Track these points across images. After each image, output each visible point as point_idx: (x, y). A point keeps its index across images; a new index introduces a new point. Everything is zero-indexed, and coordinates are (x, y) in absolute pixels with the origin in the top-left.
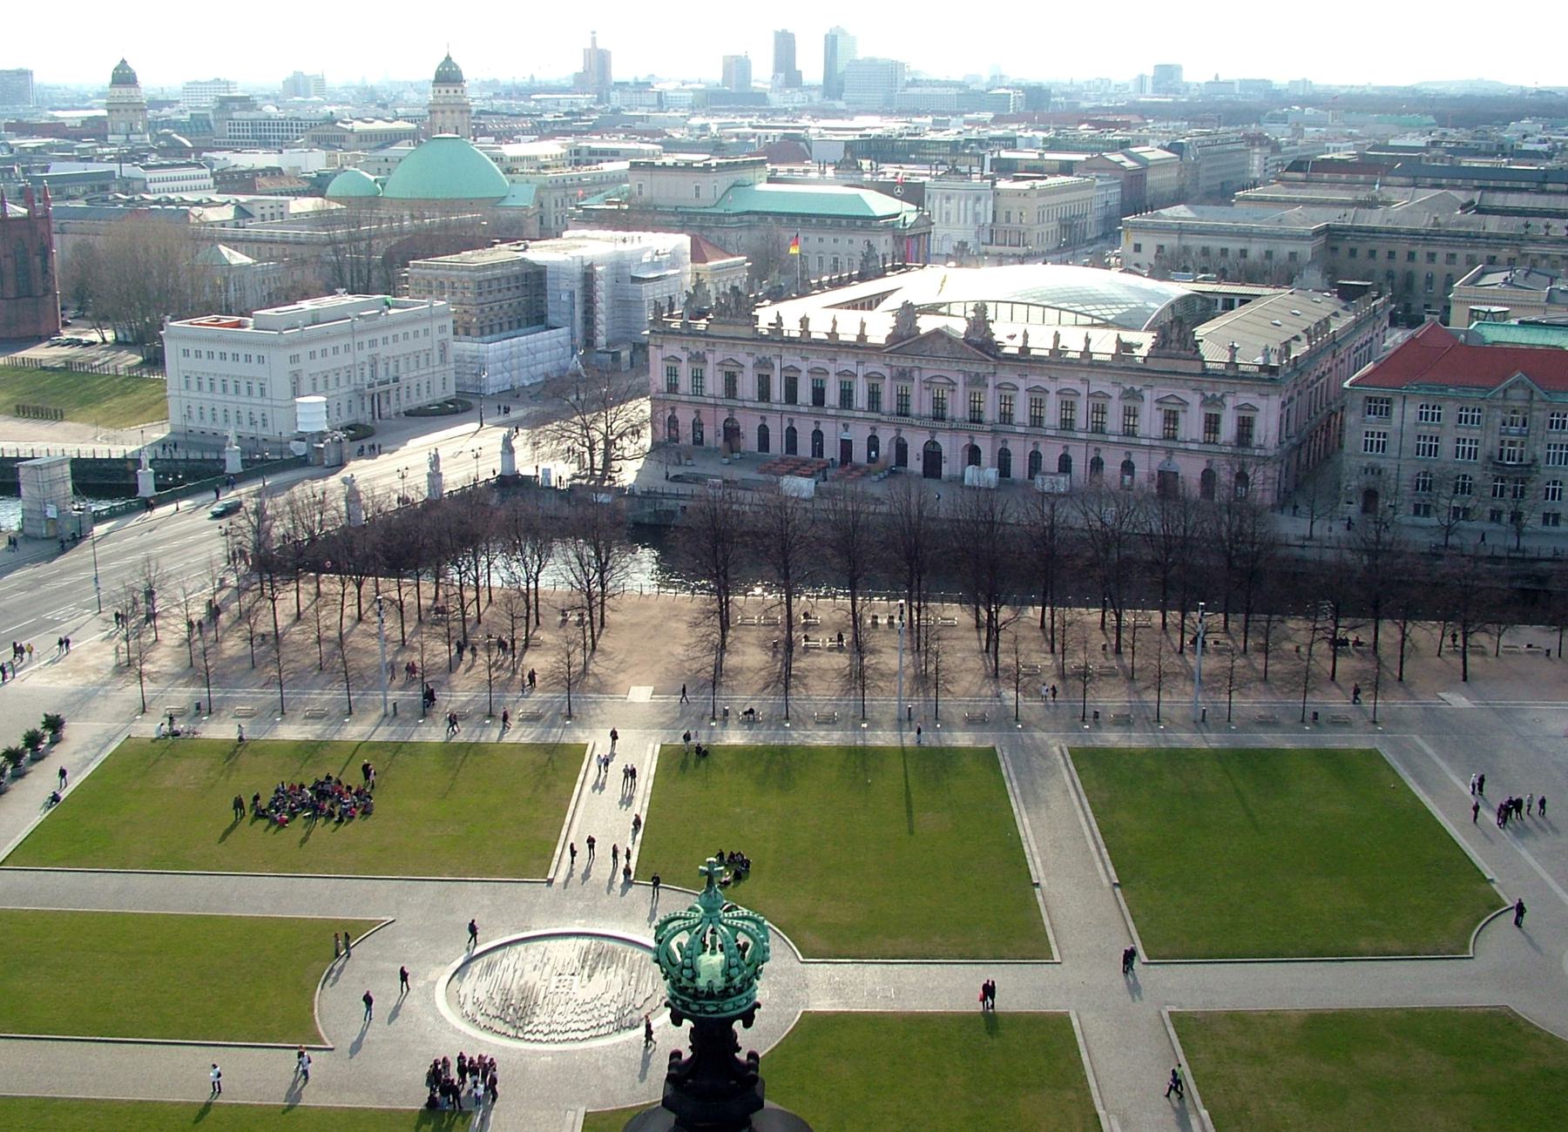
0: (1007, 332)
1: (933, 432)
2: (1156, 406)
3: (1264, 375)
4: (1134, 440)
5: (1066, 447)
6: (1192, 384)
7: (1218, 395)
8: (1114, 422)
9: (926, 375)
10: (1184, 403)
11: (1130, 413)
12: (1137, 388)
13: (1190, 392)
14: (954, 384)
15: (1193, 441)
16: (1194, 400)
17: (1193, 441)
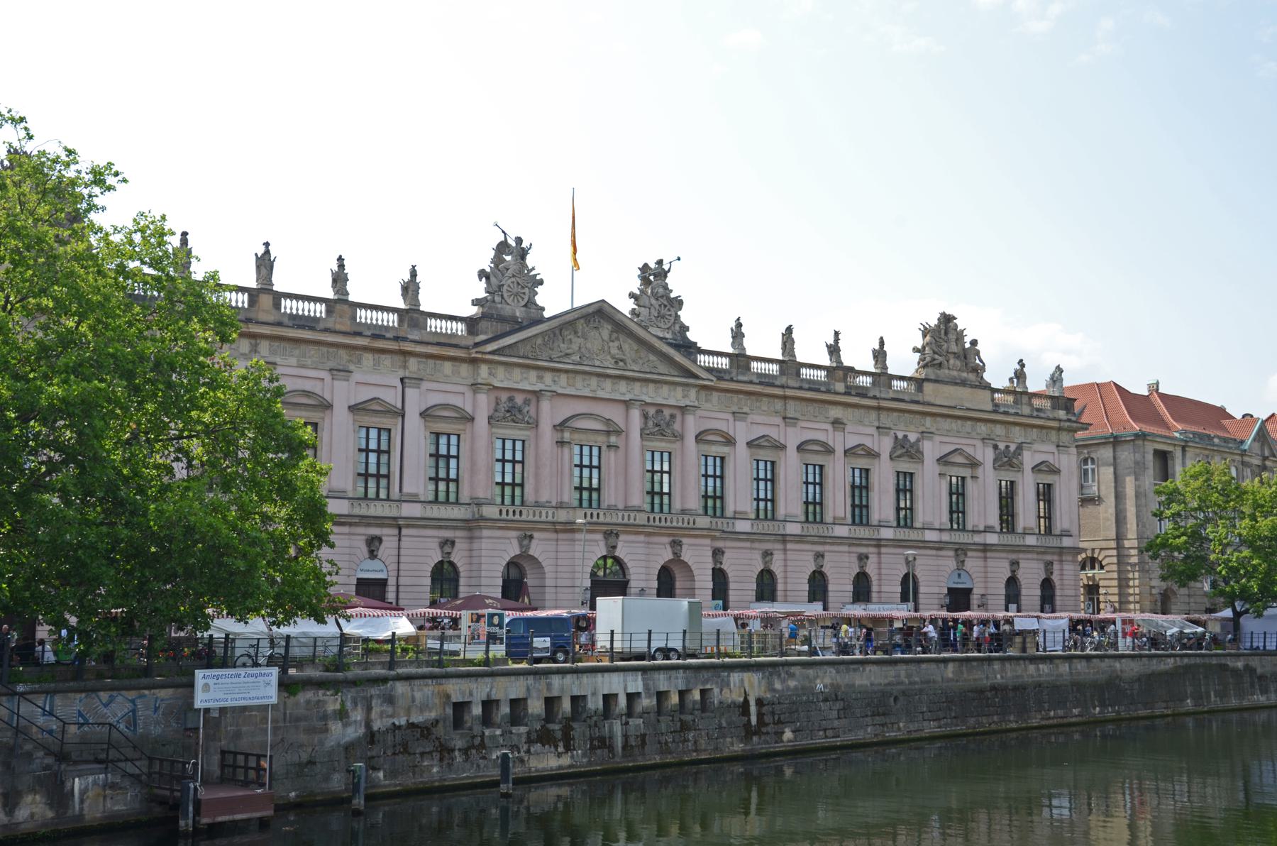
0: (708, 333)
1: (611, 535)
2: (938, 469)
3: (1062, 414)
4: (913, 535)
5: (820, 556)
6: (983, 429)
7: (1013, 448)
8: (883, 505)
9: (566, 409)
10: (974, 464)
11: (905, 485)
12: (913, 437)
13: (979, 444)
14: (618, 432)
15: (988, 529)
16: (986, 455)
17: (988, 529)
